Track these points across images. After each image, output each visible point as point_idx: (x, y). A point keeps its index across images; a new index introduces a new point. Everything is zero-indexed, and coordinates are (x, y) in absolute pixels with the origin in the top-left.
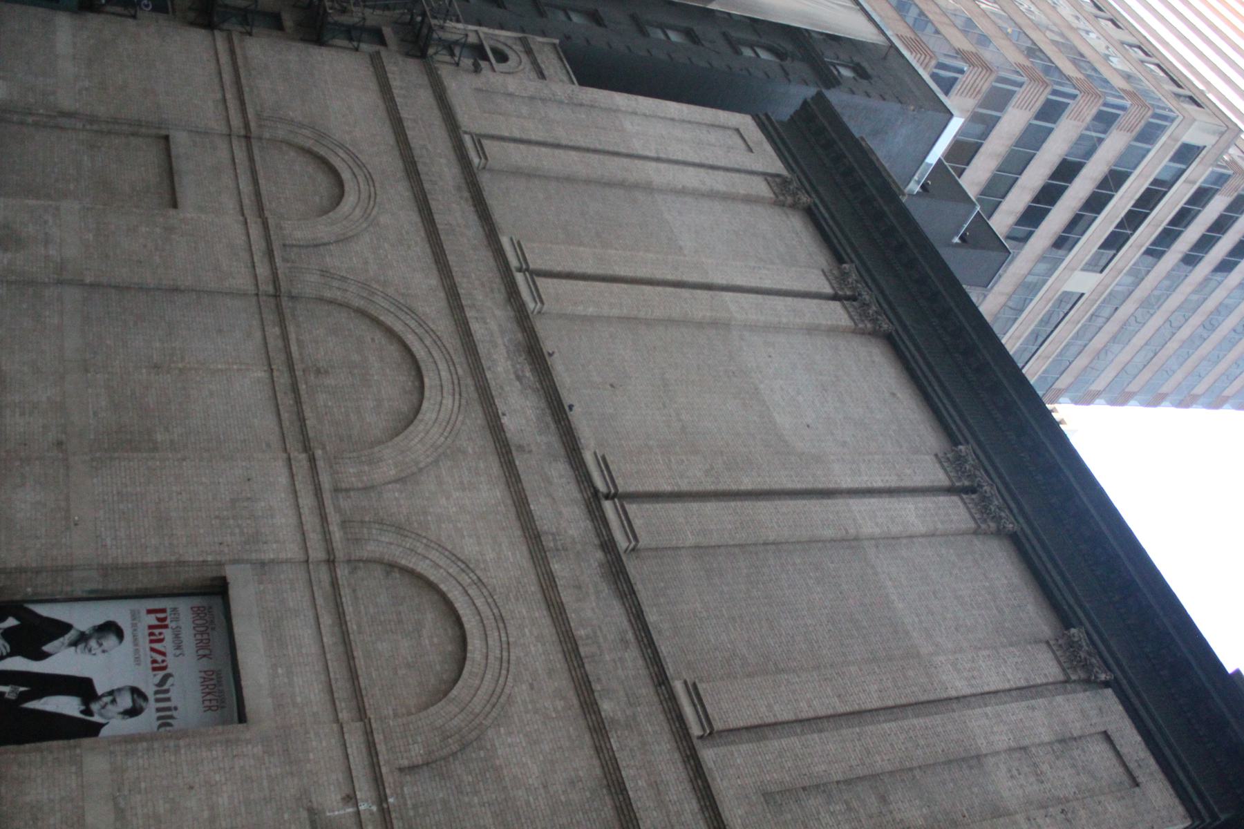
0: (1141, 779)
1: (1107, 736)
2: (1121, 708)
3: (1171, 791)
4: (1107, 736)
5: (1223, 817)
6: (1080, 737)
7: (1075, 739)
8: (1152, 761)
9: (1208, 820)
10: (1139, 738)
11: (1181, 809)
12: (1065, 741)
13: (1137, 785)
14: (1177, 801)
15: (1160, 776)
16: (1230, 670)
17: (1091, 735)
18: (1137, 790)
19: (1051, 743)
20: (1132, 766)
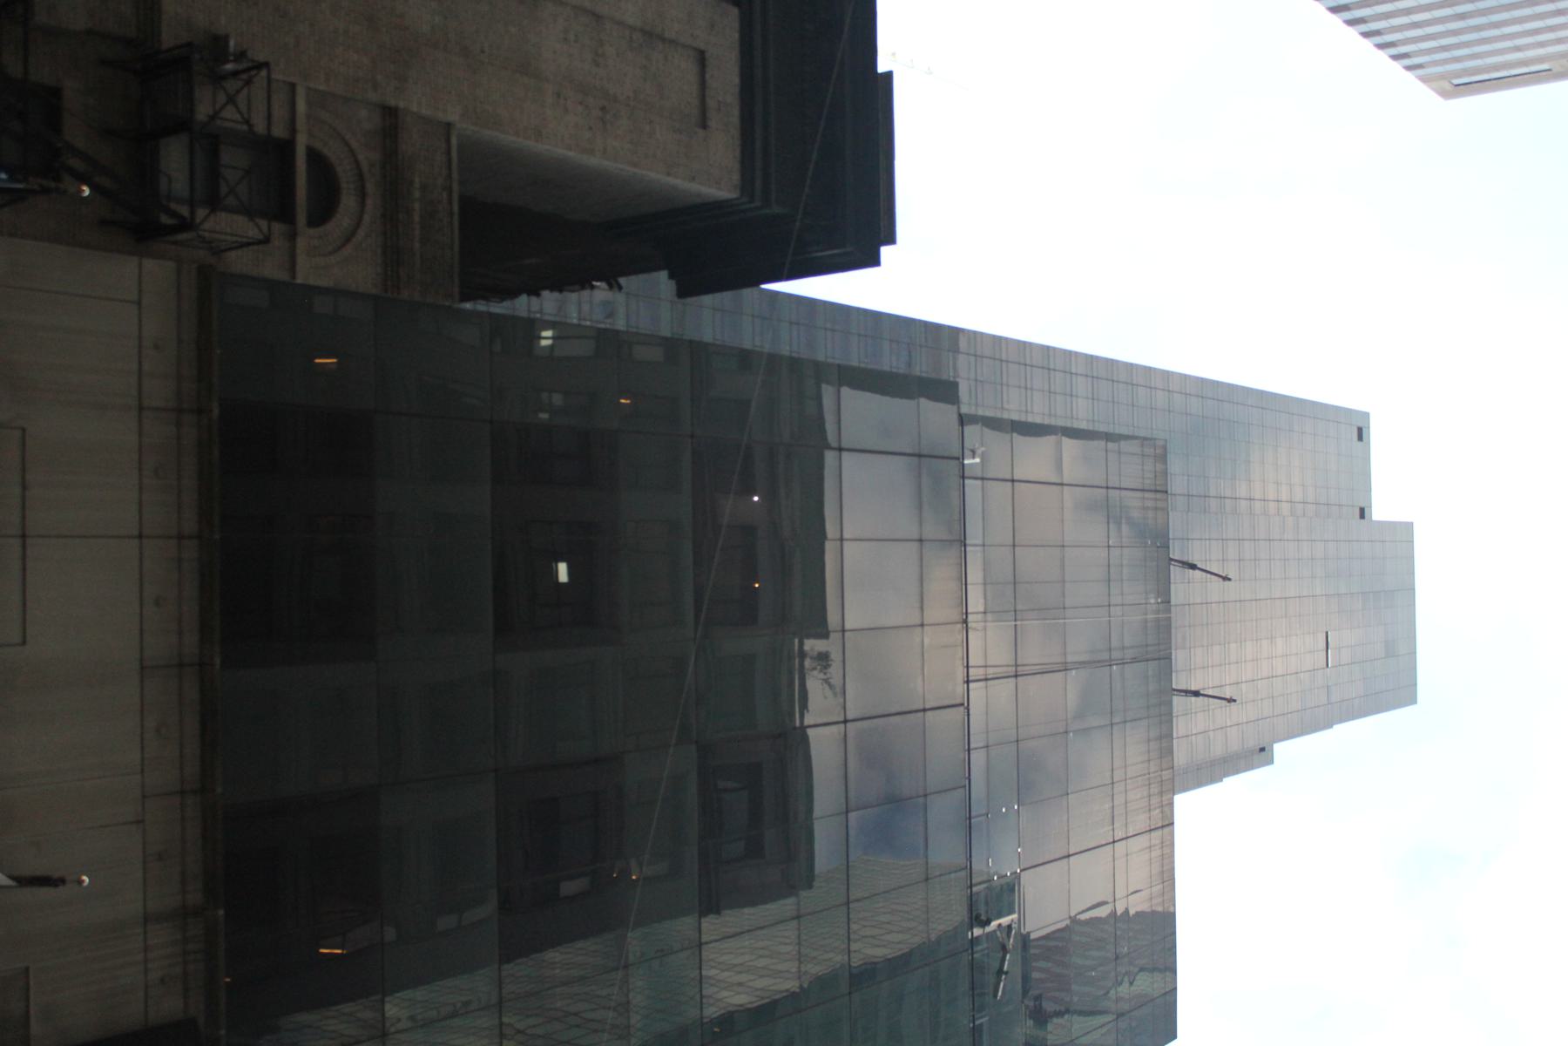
0: (712, 123)
1: (702, 58)
2: (737, 36)
3: (738, 153)
4: (702, 58)
5: (777, 210)
6: (672, 42)
7: (663, 40)
8: (736, 112)
9: (758, 204)
10: (737, 80)
11: (736, 177)
12: (651, 36)
13: (704, 126)
14: (737, 166)
15: (735, 132)
16: (882, 68)
17: (684, 46)
18: (701, 132)
19: (632, 29)
20: (711, 103)
